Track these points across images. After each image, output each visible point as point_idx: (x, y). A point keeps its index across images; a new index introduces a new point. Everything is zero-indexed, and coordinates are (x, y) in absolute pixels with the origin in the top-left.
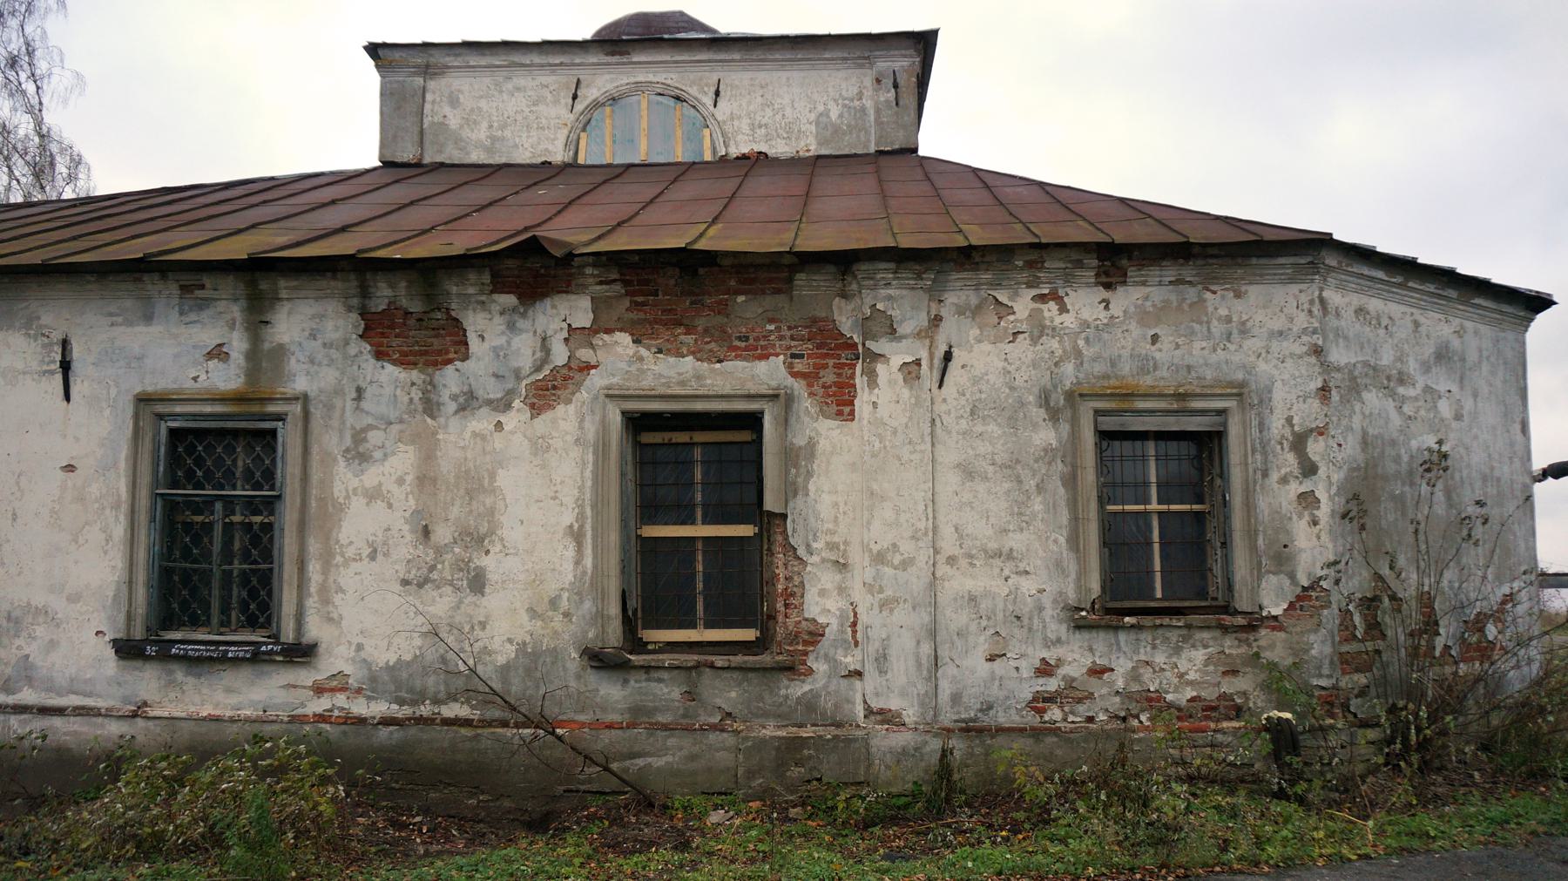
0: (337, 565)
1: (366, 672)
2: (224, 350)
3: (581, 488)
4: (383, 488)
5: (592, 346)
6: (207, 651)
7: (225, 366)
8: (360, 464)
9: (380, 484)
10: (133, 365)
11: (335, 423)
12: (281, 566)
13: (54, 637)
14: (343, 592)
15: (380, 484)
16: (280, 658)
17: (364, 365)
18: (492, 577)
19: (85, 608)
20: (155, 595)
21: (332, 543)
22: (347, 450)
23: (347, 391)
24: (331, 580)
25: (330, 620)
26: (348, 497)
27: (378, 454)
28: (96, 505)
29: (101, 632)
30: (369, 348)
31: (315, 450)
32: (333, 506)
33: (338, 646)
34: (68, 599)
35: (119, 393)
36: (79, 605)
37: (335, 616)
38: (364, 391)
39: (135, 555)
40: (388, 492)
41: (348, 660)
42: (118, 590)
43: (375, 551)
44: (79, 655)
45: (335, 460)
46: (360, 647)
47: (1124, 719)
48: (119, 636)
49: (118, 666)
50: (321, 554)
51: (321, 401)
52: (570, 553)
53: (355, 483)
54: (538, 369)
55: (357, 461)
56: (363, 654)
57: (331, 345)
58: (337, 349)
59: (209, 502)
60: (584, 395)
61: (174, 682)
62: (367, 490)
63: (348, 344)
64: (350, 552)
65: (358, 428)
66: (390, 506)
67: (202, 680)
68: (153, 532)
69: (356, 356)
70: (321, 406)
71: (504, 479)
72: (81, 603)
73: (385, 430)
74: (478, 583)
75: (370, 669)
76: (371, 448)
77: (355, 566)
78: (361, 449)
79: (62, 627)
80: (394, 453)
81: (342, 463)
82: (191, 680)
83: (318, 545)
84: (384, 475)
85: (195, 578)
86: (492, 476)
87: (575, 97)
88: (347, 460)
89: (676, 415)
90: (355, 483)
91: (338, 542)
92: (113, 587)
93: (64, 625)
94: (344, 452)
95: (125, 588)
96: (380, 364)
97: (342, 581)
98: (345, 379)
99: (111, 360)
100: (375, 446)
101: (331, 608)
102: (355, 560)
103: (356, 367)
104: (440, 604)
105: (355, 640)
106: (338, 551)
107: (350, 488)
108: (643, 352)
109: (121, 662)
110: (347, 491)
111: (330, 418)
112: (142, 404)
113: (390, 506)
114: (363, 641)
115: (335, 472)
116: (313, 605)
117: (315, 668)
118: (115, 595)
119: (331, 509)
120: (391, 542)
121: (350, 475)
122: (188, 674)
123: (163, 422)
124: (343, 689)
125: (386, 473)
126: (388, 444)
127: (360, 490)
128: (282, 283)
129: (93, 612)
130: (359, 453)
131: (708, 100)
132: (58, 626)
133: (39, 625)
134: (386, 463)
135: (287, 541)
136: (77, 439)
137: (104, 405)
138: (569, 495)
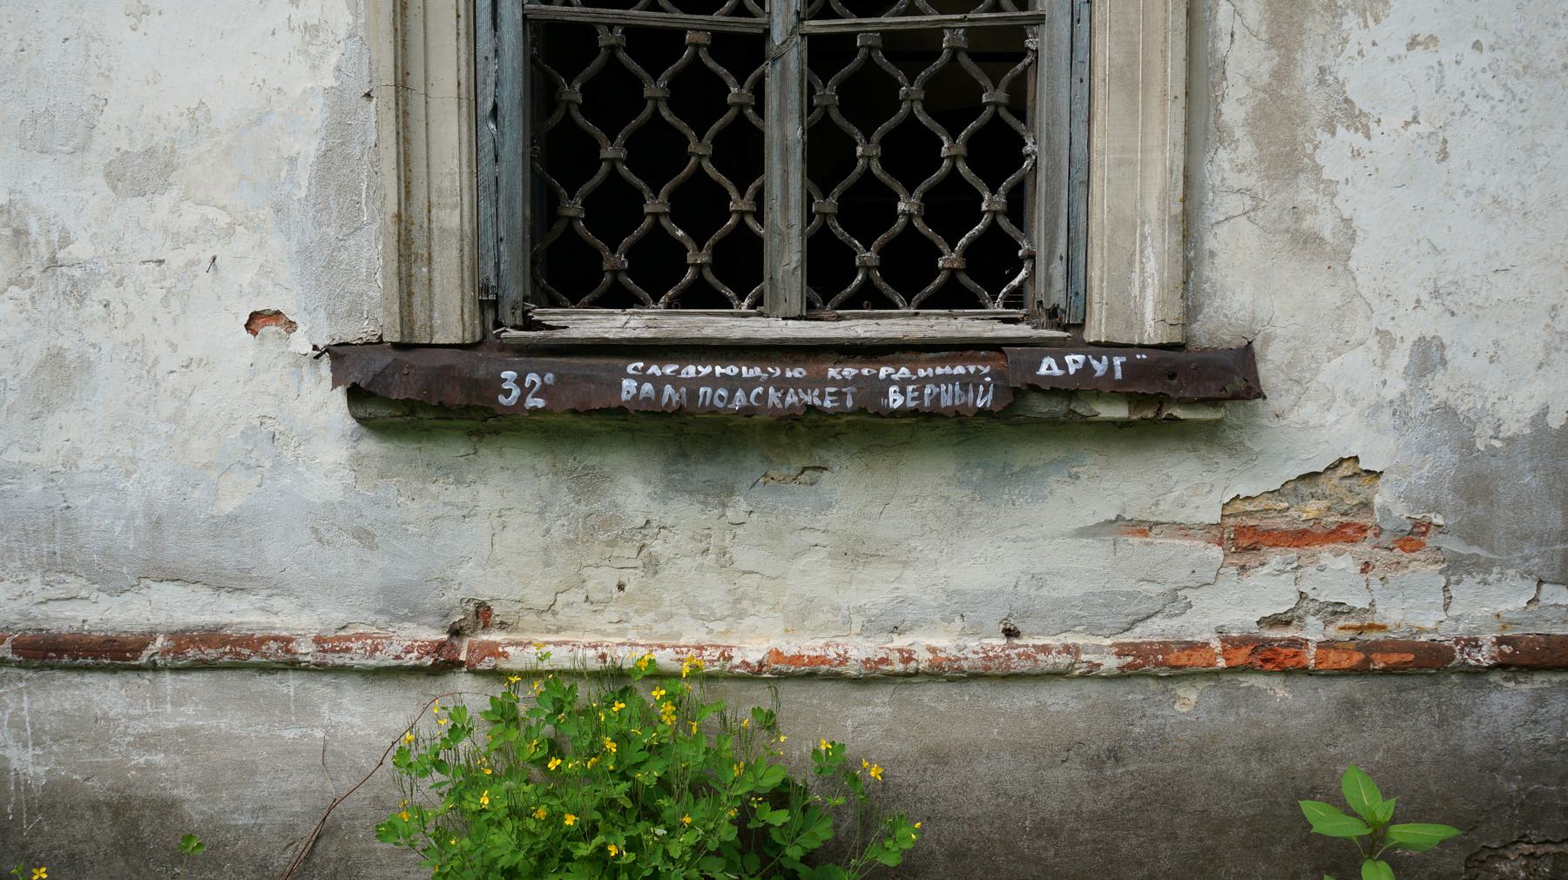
1: (1447, 457)
6: (783, 384)
13: (68, 342)
14: (1355, 118)
16: (1120, 412)
19: (191, 216)
24: (1307, 70)
25: (1306, 242)
33: (1334, 351)
34: (113, 176)
36: (164, 202)
37: (1324, 223)
41: (1377, 408)
42: (339, 127)
44: (176, 418)
46: (1428, 357)
48: (356, 331)
49: (357, 461)
56: (1441, 387)
61: (606, 525)
67: (739, 507)
72: (175, 192)
75: (1466, 446)
79: (97, 295)
82: (686, 514)
92: (317, 114)
93: (106, 290)
95: (375, 123)
97: (1355, 79)
101: (1306, 194)
105: (1411, 327)
109: (371, 446)
114: (1446, 330)
116: (1235, 181)
117: (1233, 450)
118: (326, 155)
122: (673, 487)
124: (1343, 534)
129: (230, 230)
132: (77, 293)
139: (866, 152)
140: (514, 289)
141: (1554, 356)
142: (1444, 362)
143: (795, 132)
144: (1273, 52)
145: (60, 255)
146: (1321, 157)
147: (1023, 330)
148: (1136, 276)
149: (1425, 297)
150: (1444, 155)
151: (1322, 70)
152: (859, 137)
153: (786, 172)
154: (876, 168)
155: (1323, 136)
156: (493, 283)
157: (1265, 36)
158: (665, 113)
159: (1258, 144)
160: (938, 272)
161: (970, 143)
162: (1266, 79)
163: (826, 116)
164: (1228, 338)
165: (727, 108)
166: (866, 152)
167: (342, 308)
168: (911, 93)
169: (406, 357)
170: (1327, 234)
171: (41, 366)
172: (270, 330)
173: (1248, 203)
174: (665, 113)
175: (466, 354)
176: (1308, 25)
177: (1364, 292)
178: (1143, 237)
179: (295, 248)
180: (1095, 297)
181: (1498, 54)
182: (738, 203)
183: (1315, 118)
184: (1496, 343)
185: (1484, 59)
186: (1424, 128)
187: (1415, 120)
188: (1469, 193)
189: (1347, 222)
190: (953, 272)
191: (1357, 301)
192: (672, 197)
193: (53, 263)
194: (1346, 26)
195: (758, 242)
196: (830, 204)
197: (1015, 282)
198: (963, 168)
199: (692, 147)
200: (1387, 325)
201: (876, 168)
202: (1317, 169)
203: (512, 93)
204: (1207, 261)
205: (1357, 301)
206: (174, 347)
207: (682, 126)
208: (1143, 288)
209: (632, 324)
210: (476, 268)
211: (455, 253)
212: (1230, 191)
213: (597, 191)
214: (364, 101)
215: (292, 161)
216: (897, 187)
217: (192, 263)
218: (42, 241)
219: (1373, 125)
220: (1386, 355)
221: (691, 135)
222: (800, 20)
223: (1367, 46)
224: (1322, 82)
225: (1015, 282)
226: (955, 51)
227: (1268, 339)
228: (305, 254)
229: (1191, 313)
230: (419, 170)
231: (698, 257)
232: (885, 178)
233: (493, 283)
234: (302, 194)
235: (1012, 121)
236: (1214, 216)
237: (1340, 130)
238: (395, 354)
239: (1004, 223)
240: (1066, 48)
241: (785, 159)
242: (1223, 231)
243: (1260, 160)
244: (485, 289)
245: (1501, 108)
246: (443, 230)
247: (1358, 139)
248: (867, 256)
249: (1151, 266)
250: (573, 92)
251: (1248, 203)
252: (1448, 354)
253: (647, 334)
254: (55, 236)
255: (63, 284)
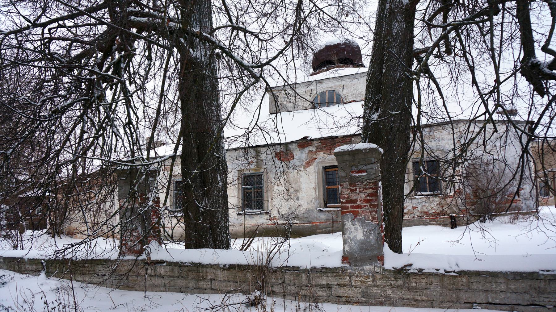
3: (315, 180)
5: (316, 155)
18: (300, 197)
47: (421, 217)
52: (314, 192)
54: (306, 160)
59: (251, 188)
60: (315, 164)
71: (301, 180)
74: (298, 199)
82: (250, 219)
86: (300, 179)
87: (311, 93)
89: (332, 166)
104: (291, 203)
108: (325, 155)
128: (261, 149)
131: (341, 90)
138: (313, 181)
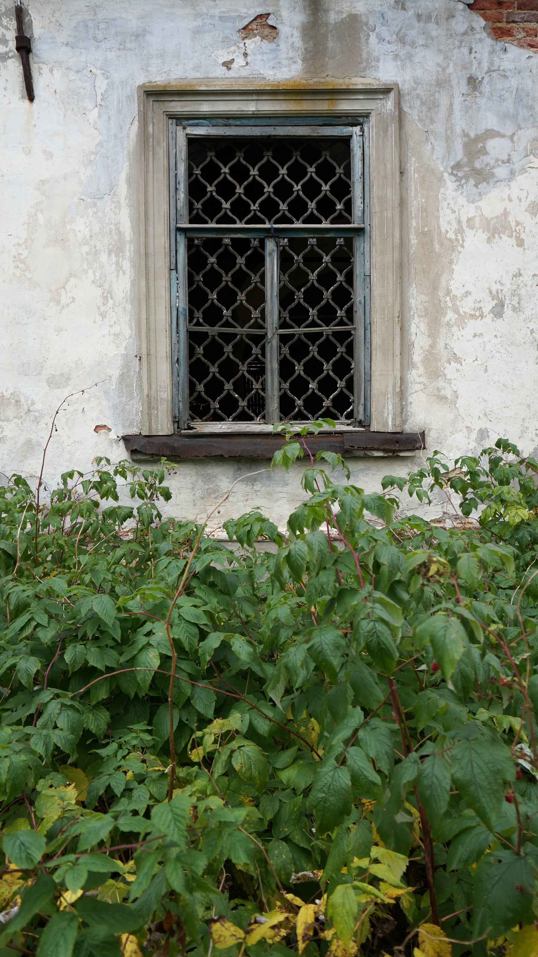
0: (448, 324)
2: (270, 22)
4: (511, 218)
7: (273, 46)
8: (476, 186)
9: (506, 213)
10: (128, 45)
11: (440, 127)
12: (368, 327)
14: (457, 359)
15: (506, 213)
17: (477, 47)
20: (182, 373)
21: (441, 294)
22: (458, 166)
23: (454, 82)
24: (441, 345)
25: (442, 399)
26: (460, 231)
27: (501, 172)
28: (86, 249)
29: (104, 427)
30: (483, 23)
31: (412, 166)
32: (441, 245)
34: (49, 383)
35: (111, 85)
37: (448, 393)
38: (481, 82)
39: (152, 317)
40: (518, 223)
42: (126, 366)
43: (501, 304)
45: (440, 179)
48: (134, 431)
50: (426, 309)
51: (418, 96)
53: (469, 211)
55: (472, 182)
57: (429, 18)
58: (437, 23)
62: (488, 221)
63: (453, 17)
64: (467, 306)
65: (472, 135)
66: (520, 243)
68: (174, 281)
69: (465, 34)
70: (419, 103)
73: (511, 138)
76: (492, 163)
77: (473, 326)
78: (478, 165)
80: (523, 170)
81: (450, 184)
83: (423, 298)
84: (510, 200)
85: (228, 349)
88: (459, 180)
90: (469, 211)
91: (448, 292)
92: (119, 362)
94: (453, 168)
96: (499, 45)
98: (451, 65)
99: (95, 38)
100: (497, 160)
101: (441, 383)
102: (473, 316)
103: (465, 51)
106: (450, 304)
107: (464, 219)
110: (459, 222)
111: (432, 121)
112: (151, 99)
113: (520, 243)
115: (440, 197)
116: (418, 380)
118: (122, 375)
119: (437, 247)
120: (523, 292)
121: (462, 200)
123: (180, 128)
125: (514, 198)
126: (515, 158)
127: (477, 220)
130: (474, 169)
133: (8, 420)
134: (513, 184)
135: (376, 291)
136: (49, 155)
137: (88, 104)
139: (299, 369)
140: (185, 416)
141: (524, 434)
142: (488, 436)
143: (276, 366)
144: (430, 339)
145: (31, 408)
146: (446, 372)
147: (351, 428)
148: (386, 410)
149: (481, 416)
150: (486, 371)
151: (446, 344)
152: (296, 363)
153: (272, 378)
154: (302, 373)
155: (447, 365)
156: (177, 415)
157: (427, 334)
158: (231, 357)
159: (425, 368)
160: (323, 407)
161: (334, 365)
162: (428, 348)
163: (285, 356)
164: (417, 430)
165: (252, 355)
166: (299, 369)
167: (127, 424)
168: (314, 350)
169: (151, 440)
170: (449, 397)
171: (24, 444)
172: (103, 431)
173: (422, 387)
174: (231, 357)
175: (169, 438)
176: (441, 330)
177: (461, 414)
178: (388, 398)
179: (111, 405)
180: (374, 417)
181: (503, 339)
182: (256, 386)
183: (444, 359)
184: (505, 430)
185: (499, 339)
186: (479, 362)
187: (476, 359)
188: (495, 383)
189: (455, 392)
190: (328, 407)
191: (459, 417)
192: (234, 384)
193: (29, 410)
194: (453, 330)
195: (263, 399)
196: (287, 386)
197: (349, 410)
198: (331, 373)
199: (240, 368)
200: (469, 425)
201: (302, 373)
202: (445, 375)
203: (183, 354)
204: (409, 405)
205: (459, 417)
206: (69, 437)
207: (237, 361)
208: (388, 415)
209: (223, 427)
210: (173, 410)
211: (165, 406)
212: (417, 383)
213: (208, 382)
214: (135, 358)
215: (110, 377)
216: (309, 379)
217: (76, 410)
218: (25, 404)
219: (463, 361)
220: (469, 434)
221: (240, 363)
222: (277, 330)
223: (460, 337)
224: (446, 348)
225: (349, 410)
226: (328, 335)
227: (430, 430)
228: (115, 407)
229: (404, 422)
230: (153, 379)
231: (243, 403)
232: (305, 376)
233: (177, 415)
234: (114, 387)
235: (347, 357)
236: (410, 391)
237: (452, 363)
238: (146, 440)
239: (345, 391)
240: (363, 338)
241: (272, 374)
242: (414, 396)
243: (426, 373)
244: (175, 417)
245: (504, 356)
246: (162, 399)
247: (458, 366)
248: (299, 402)
249: (391, 407)
250: (200, 350)
251: (422, 387)
252: (490, 434)
253: (229, 431)
254: (29, 402)
255: (32, 418)
